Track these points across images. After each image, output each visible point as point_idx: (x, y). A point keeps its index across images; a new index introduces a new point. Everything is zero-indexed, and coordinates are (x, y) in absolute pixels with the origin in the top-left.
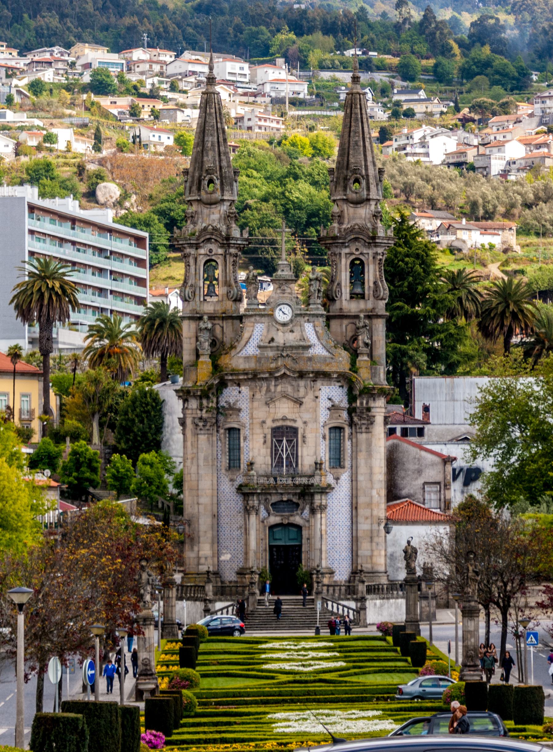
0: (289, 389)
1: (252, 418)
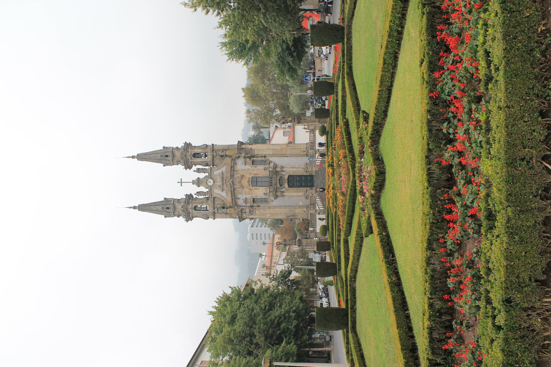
0: (238, 180)
1: (249, 194)
